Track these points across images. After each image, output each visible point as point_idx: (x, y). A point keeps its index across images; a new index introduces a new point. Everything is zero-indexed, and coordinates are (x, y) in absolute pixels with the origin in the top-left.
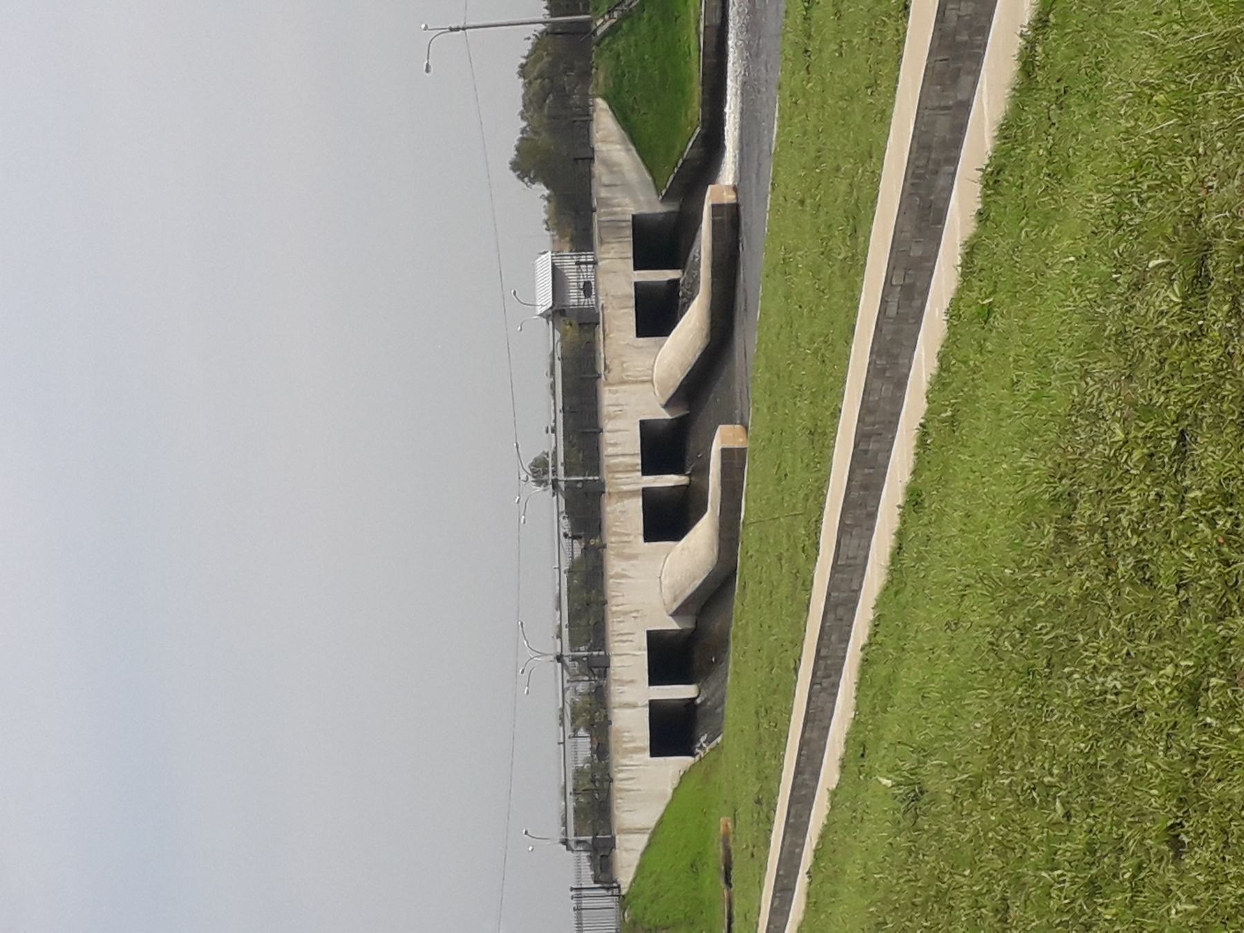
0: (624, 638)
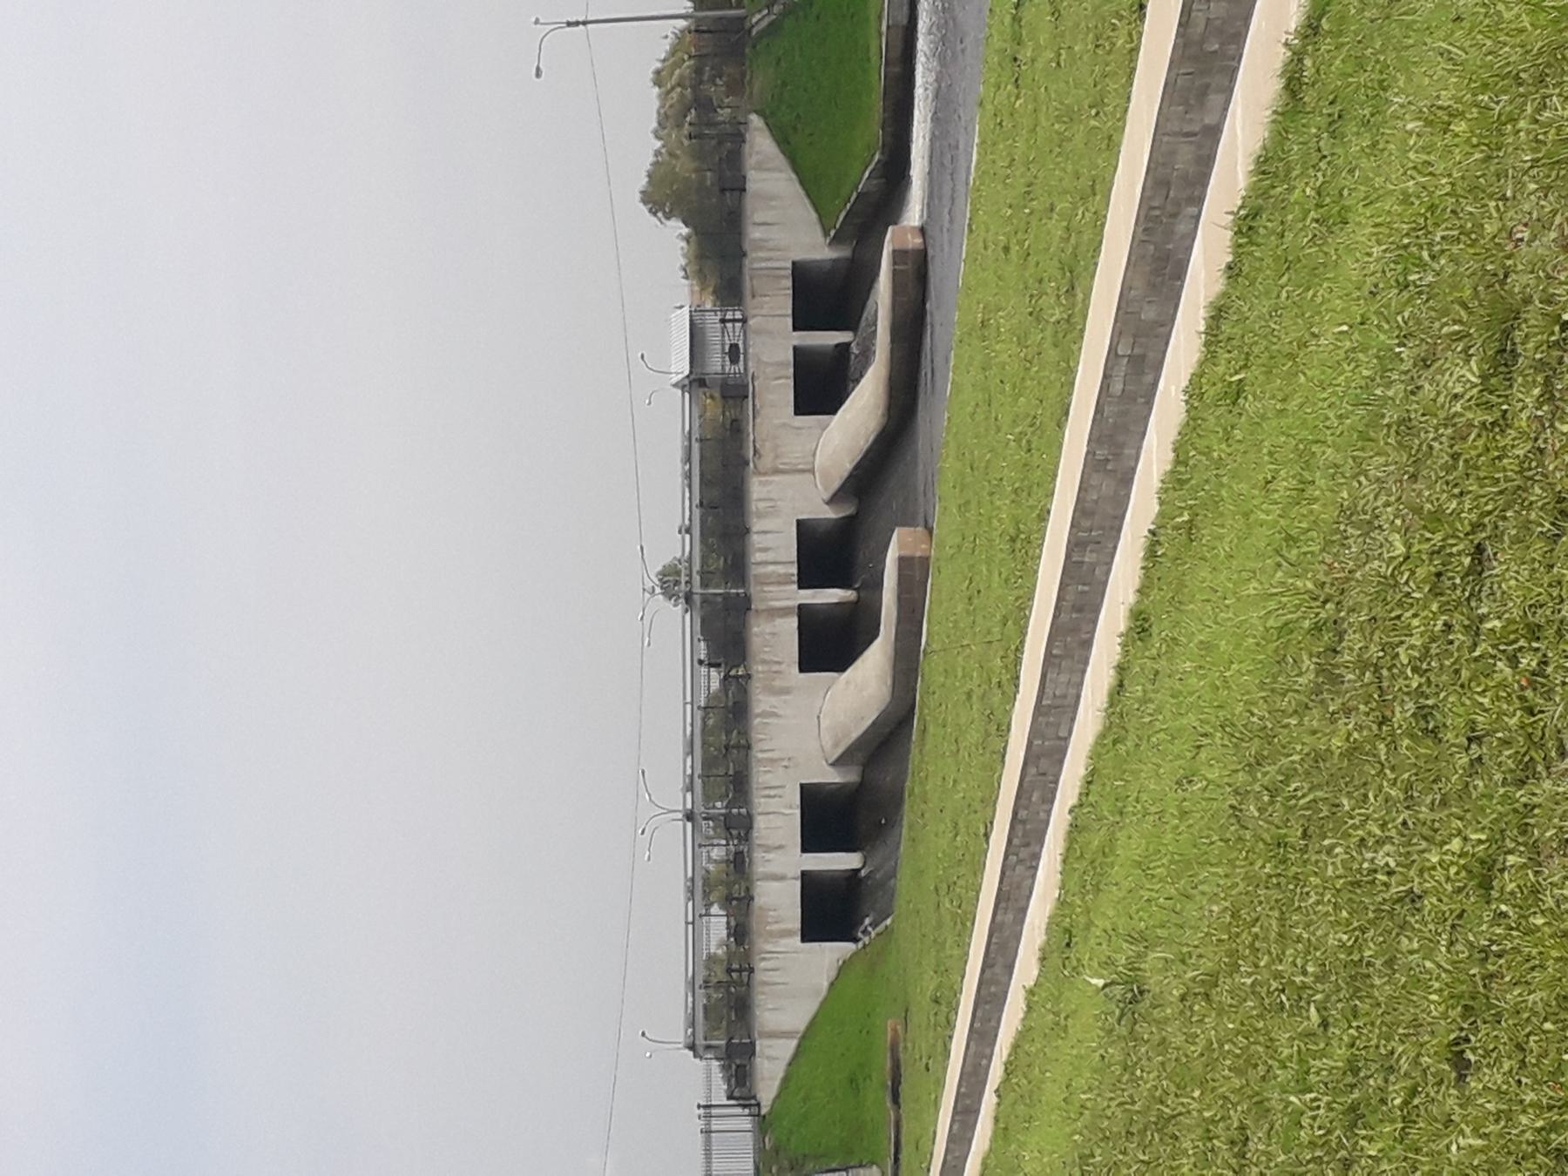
0: (772, 792)
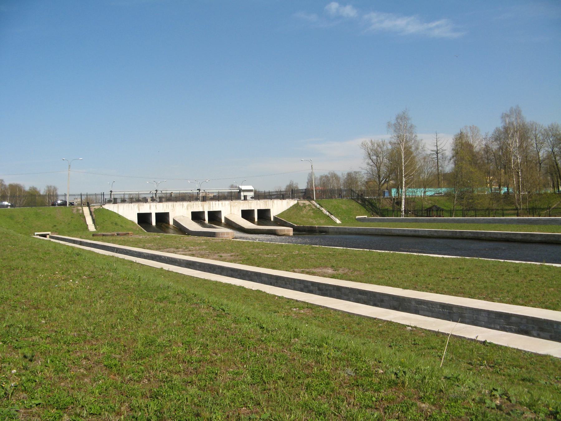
0: (167, 207)
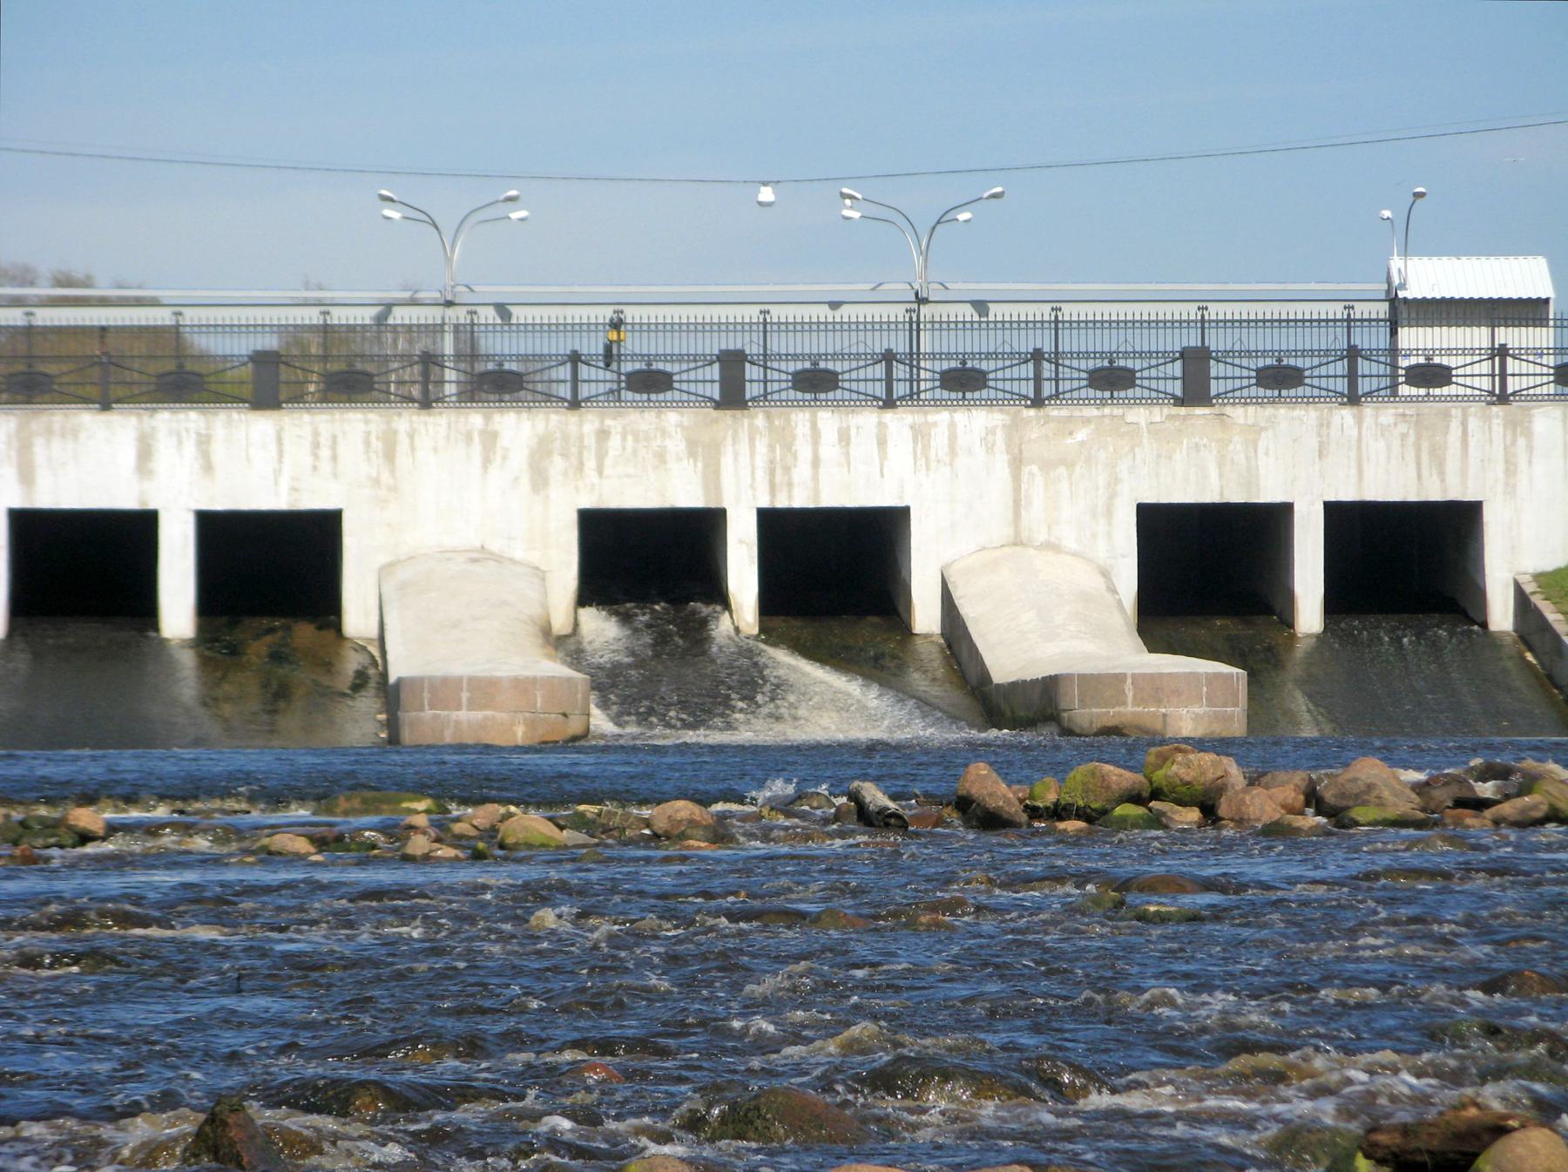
0: (325, 452)
